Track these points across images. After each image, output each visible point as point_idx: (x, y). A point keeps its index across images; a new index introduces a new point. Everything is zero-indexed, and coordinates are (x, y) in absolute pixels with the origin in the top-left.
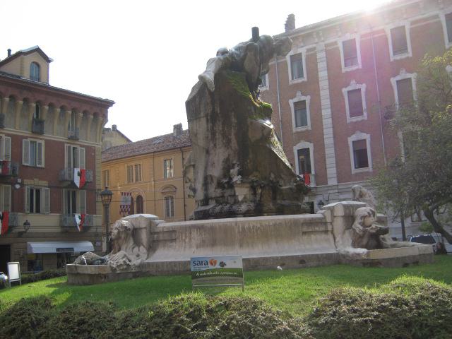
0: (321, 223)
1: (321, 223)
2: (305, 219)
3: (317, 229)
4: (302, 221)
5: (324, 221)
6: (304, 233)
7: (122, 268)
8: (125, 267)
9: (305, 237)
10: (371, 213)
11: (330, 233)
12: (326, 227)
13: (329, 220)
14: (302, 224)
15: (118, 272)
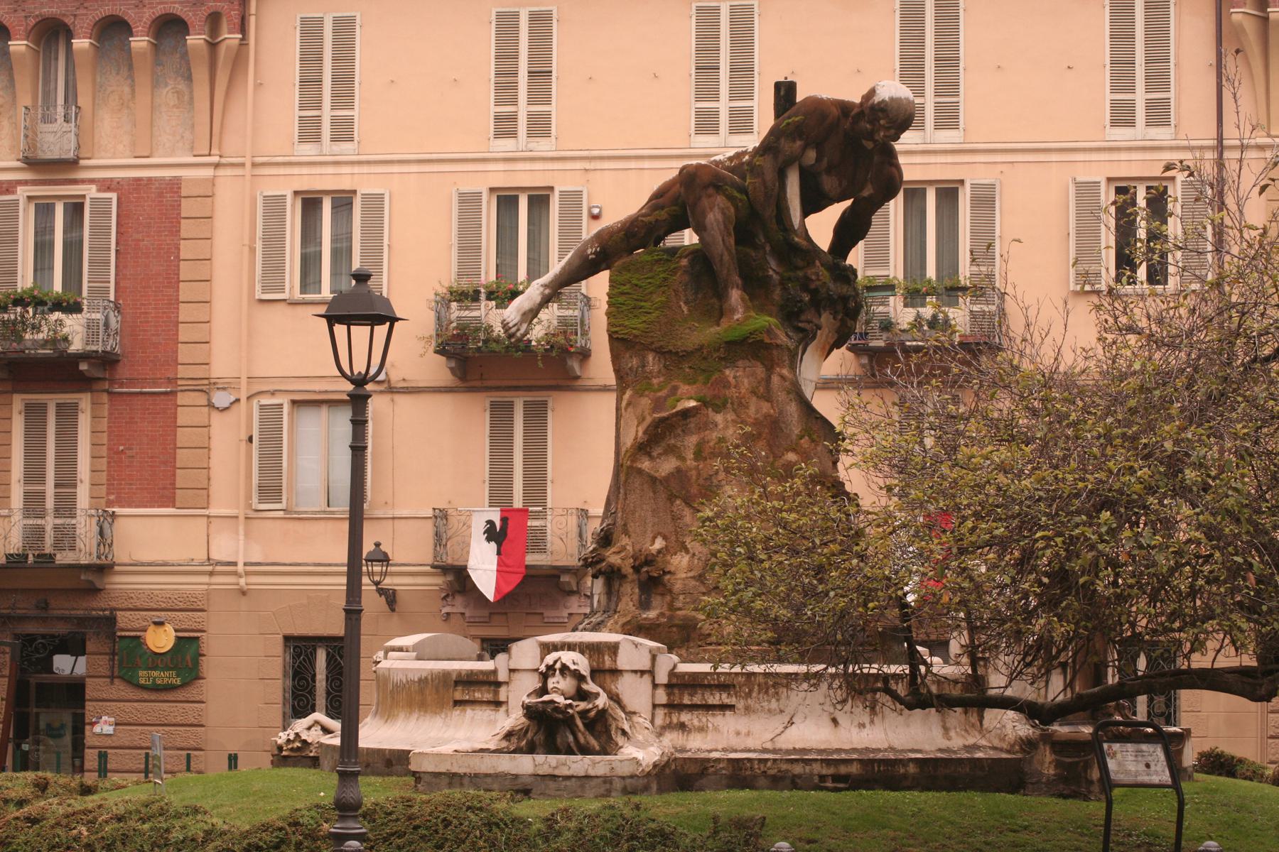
0: (490, 683)
1: (490, 683)
2: (459, 673)
3: (478, 695)
4: (454, 677)
5: (492, 678)
6: (457, 703)
7: (290, 746)
8: (298, 744)
9: (457, 712)
10: (558, 666)
11: (503, 709)
12: (496, 693)
13: (502, 676)
14: (457, 683)
15: (284, 753)
